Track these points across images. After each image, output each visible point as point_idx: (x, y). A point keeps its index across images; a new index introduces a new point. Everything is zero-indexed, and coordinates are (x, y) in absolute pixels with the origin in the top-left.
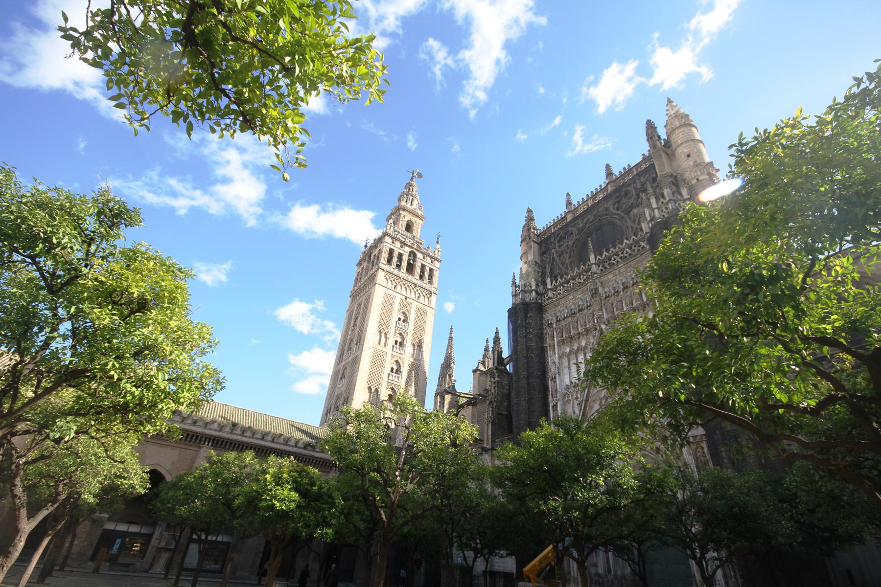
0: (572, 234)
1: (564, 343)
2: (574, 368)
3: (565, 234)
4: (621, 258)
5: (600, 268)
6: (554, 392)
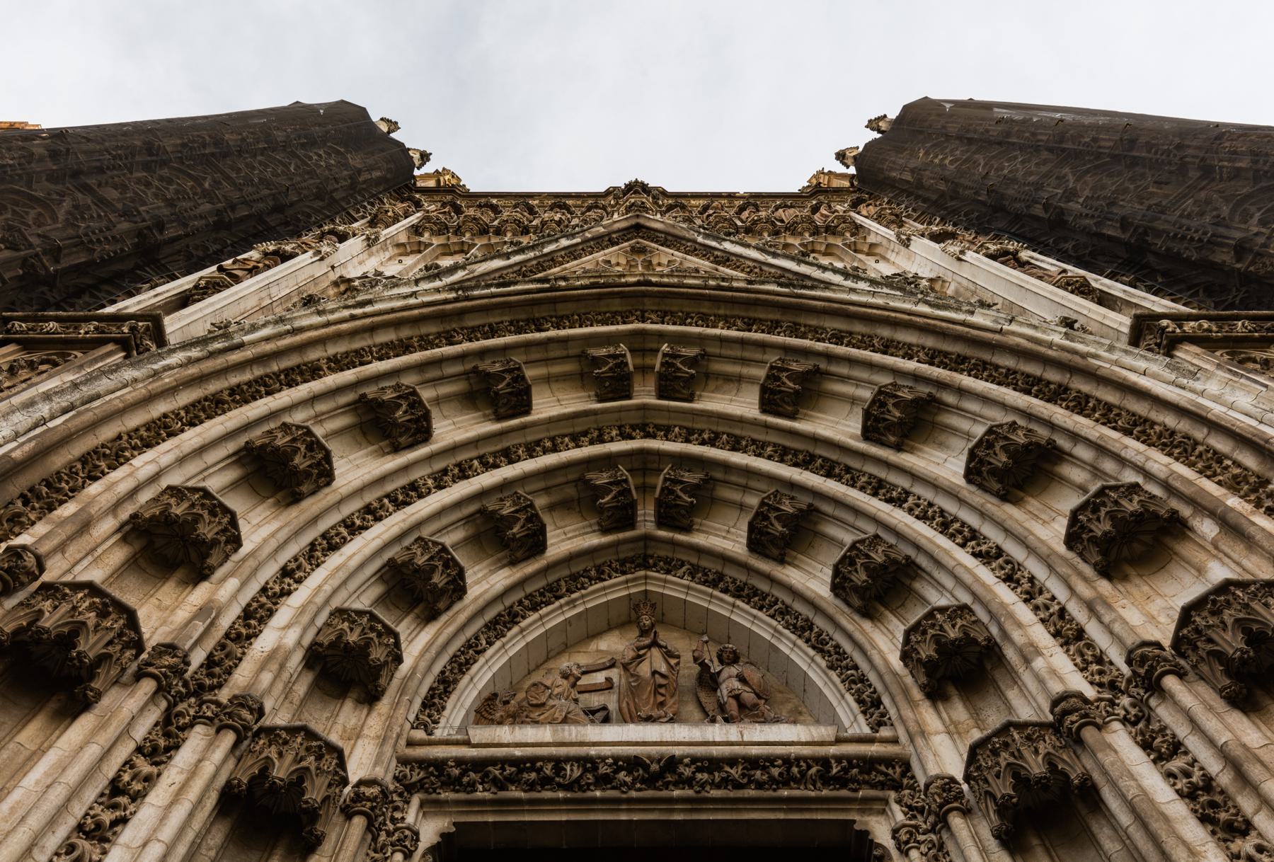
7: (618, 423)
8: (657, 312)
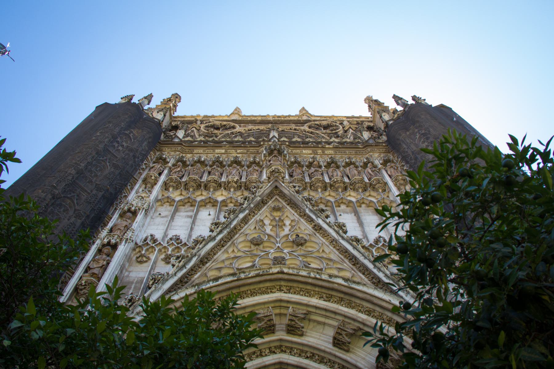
7: (269, 346)
8: (287, 286)
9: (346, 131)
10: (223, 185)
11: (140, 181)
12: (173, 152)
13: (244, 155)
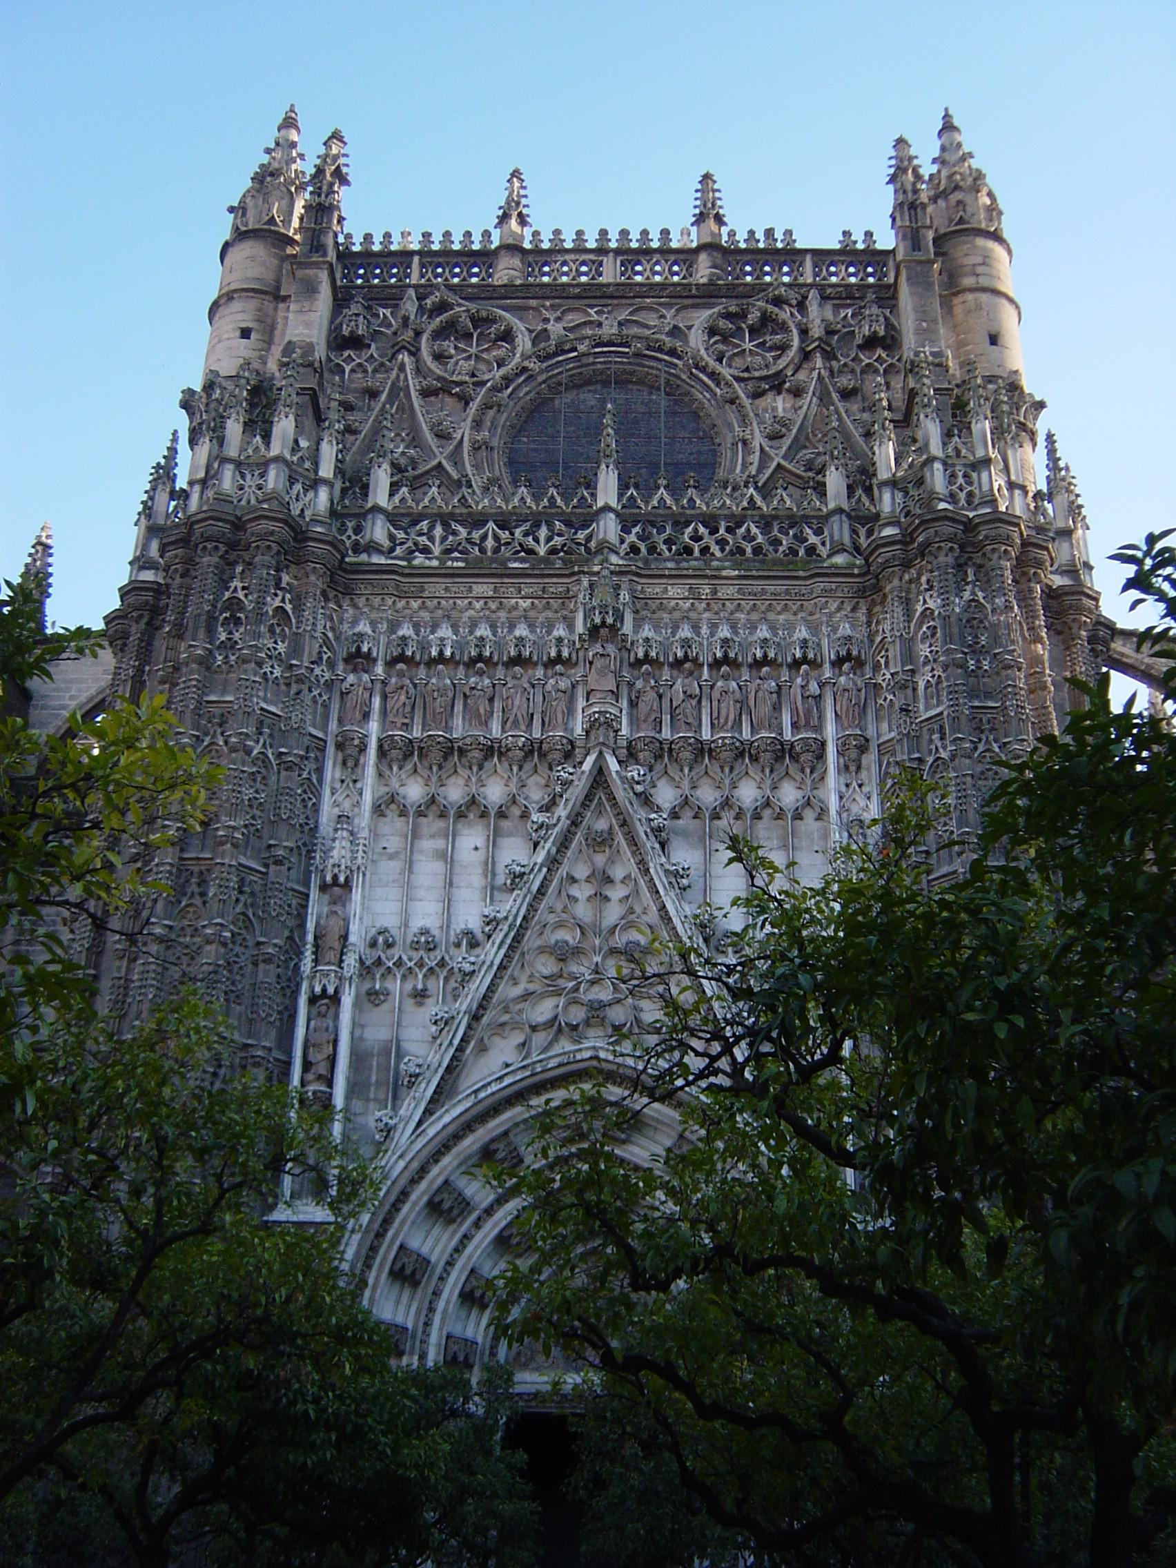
0: (507, 336)
1: (407, 756)
2: (428, 871)
3: (477, 321)
4: (722, 543)
5: (632, 538)
6: (333, 941)
9: (806, 356)
10: (496, 745)
11: (331, 749)
12: (378, 599)
13: (536, 601)
